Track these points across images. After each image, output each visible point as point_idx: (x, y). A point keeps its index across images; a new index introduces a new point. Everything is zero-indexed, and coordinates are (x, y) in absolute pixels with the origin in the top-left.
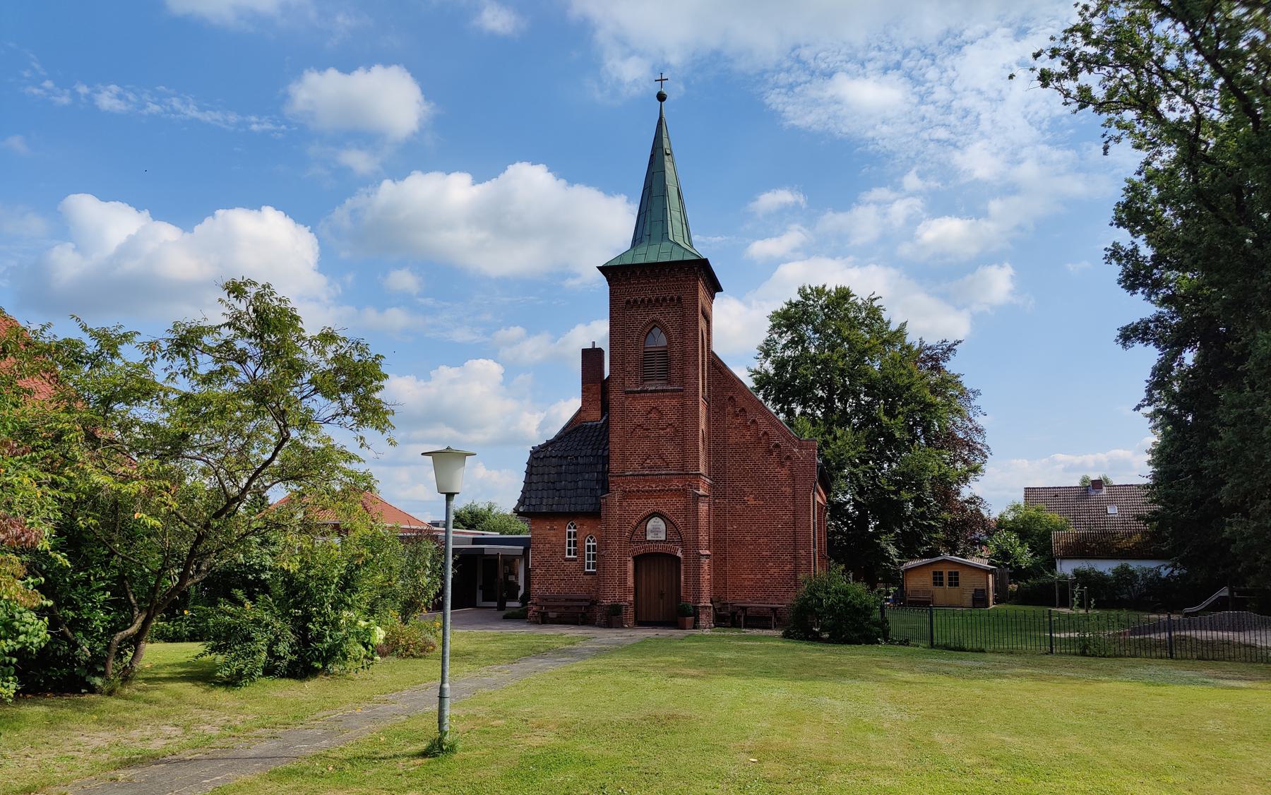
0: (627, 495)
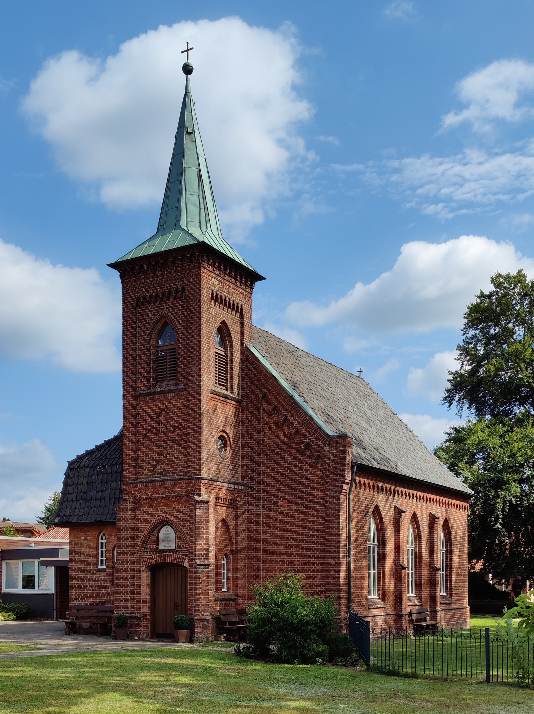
0: (138, 503)
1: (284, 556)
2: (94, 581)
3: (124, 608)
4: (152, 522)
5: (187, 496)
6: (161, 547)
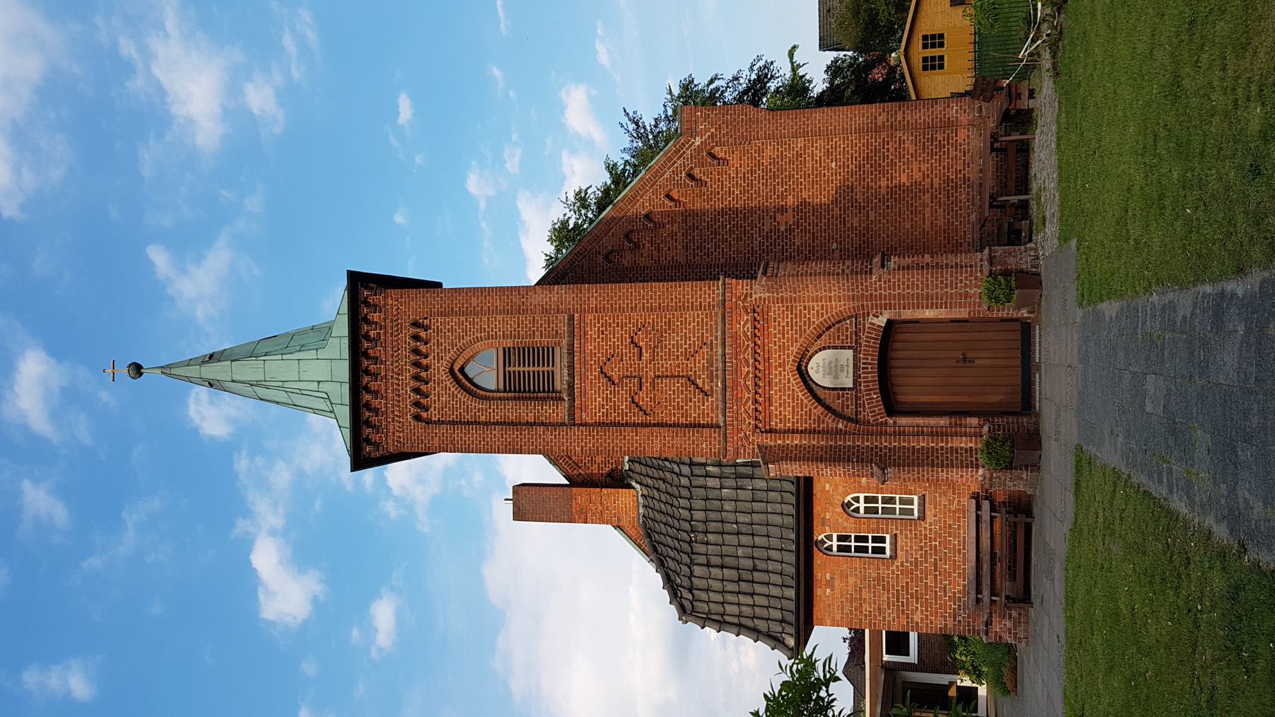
1: (872, 216)
2: (916, 566)
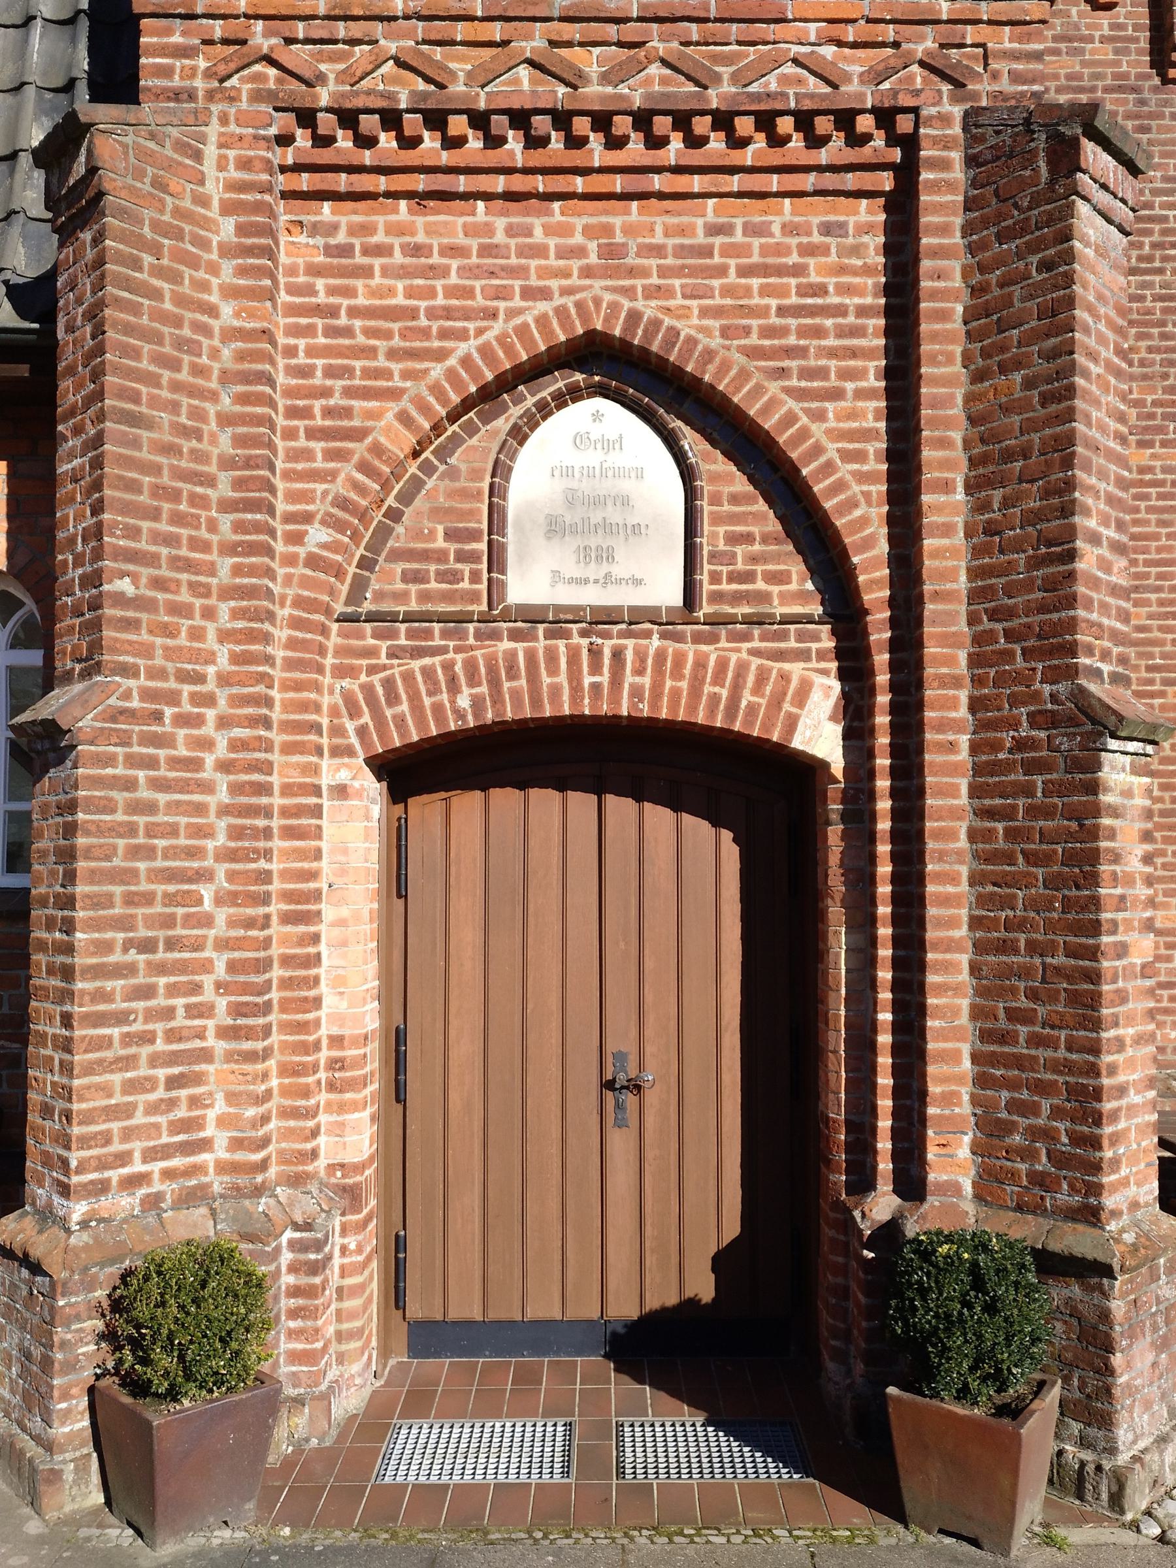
3: (165, 1152)
4: (468, 347)
5: (885, 116)
6: (526, 586)
